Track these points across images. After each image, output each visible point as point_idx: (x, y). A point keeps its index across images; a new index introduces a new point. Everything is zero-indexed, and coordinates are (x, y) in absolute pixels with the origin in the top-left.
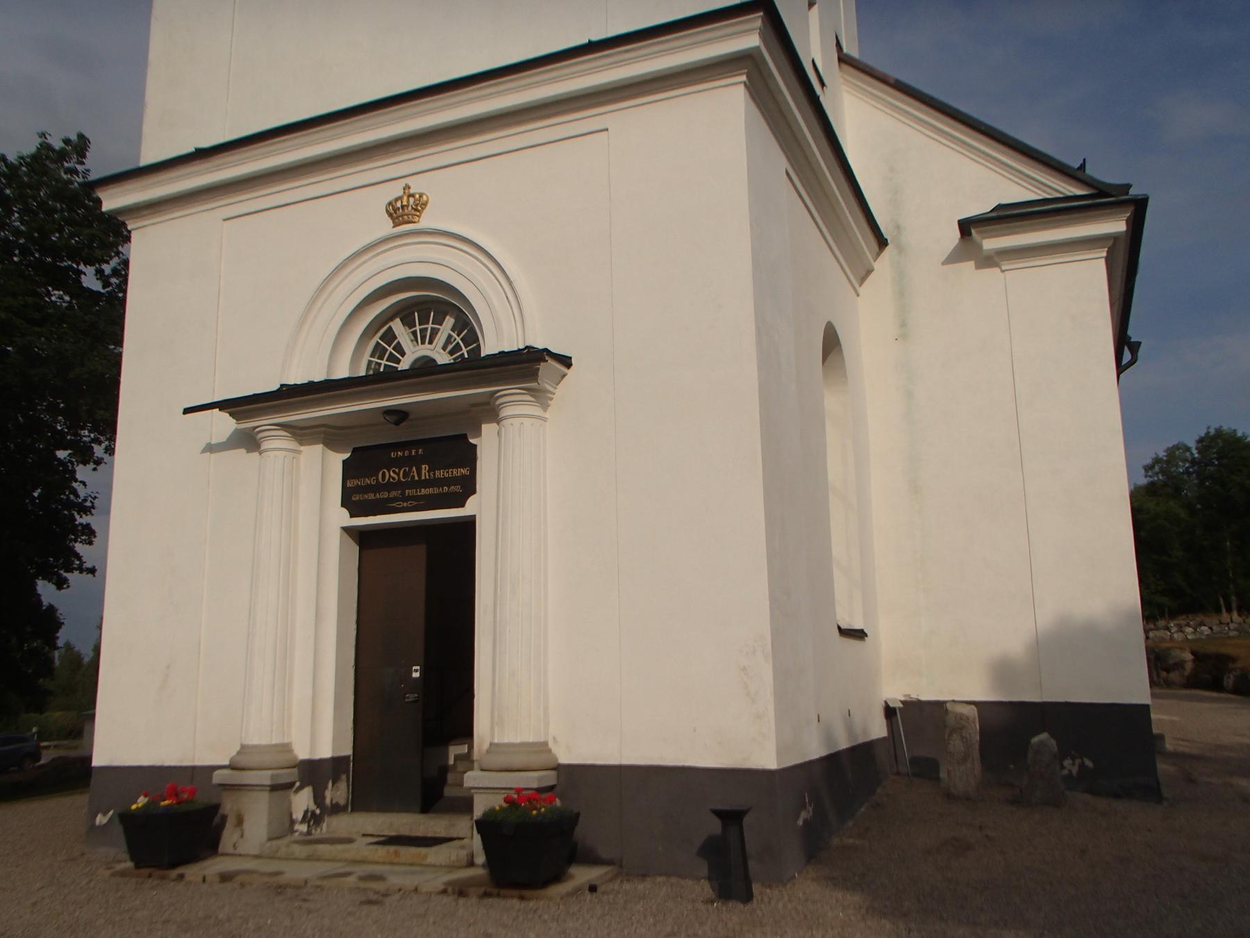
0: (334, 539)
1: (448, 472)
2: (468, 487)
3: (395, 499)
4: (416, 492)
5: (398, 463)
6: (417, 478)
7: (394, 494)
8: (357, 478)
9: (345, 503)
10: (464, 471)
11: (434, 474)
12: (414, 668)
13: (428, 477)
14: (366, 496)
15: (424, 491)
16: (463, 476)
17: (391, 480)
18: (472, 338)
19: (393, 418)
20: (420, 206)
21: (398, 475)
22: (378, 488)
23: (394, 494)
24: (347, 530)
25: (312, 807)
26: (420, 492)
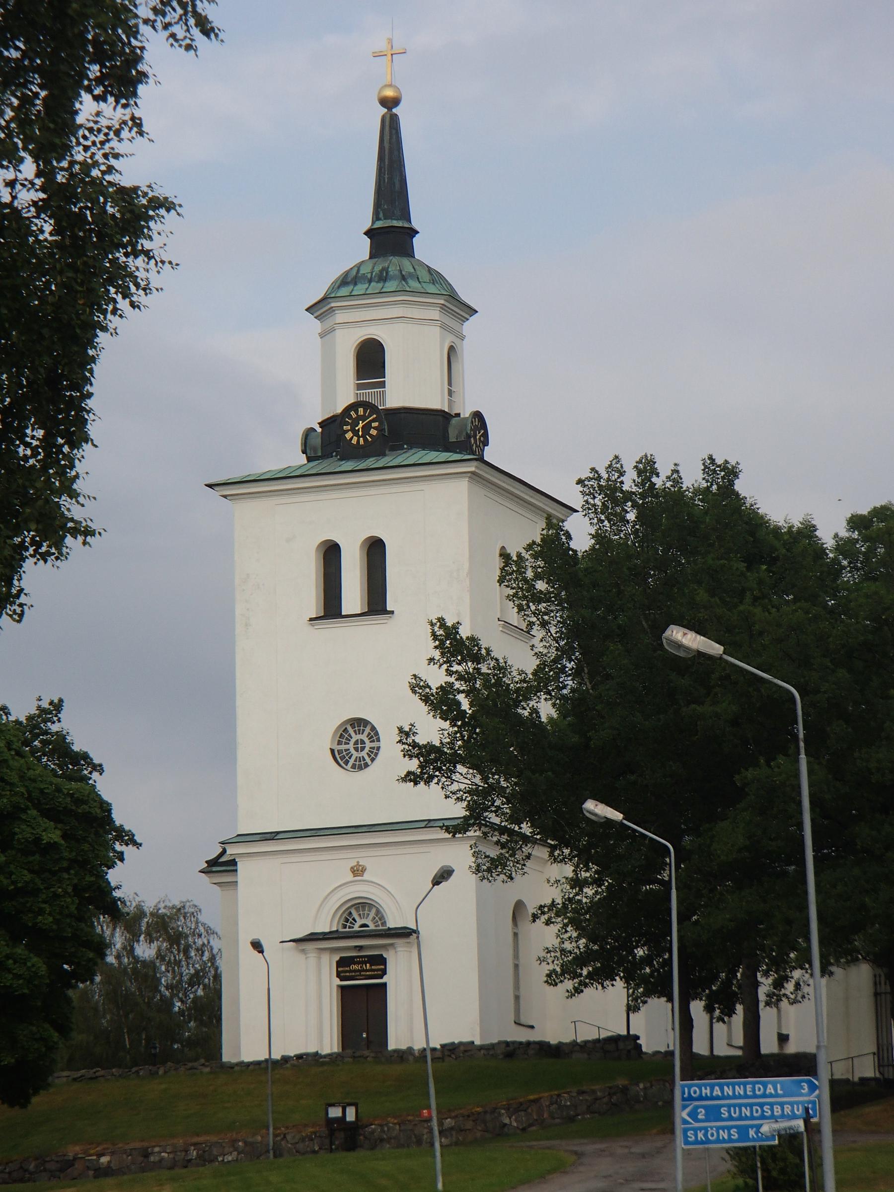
0: (335, 989)
2: (384, 972)
3: (358, 976)
5: (359, 963)
8: (343, 967)
9: (338, 976)
10: (383, 967)
15: (368, 973)
18: (382, 918)
19: (358, 949)
20: (364, 870)
24: (339, 986)
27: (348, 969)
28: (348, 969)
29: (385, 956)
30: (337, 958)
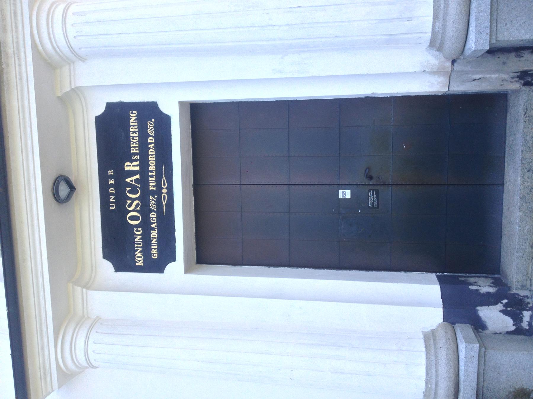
1: (133, 137)
4: (152, 176)
5: (121, 199)
6: (138, 177)
7: (153, 205)
10: (133, 117)
11: (135, 154)
12: (341, 197)
13: (138, 163)
14: (154, 241)
15: (152, 168)
16: (138, 118)
17: (138, 209)
21: (133, 200)
22: (146, 225)
23: (153, 205)
24: (188, 270)
25: (500, 306)
26: (152, 171)
27: (139, 232)
28: (139, 232)
29: (100, 110)
30: (108, 266)
